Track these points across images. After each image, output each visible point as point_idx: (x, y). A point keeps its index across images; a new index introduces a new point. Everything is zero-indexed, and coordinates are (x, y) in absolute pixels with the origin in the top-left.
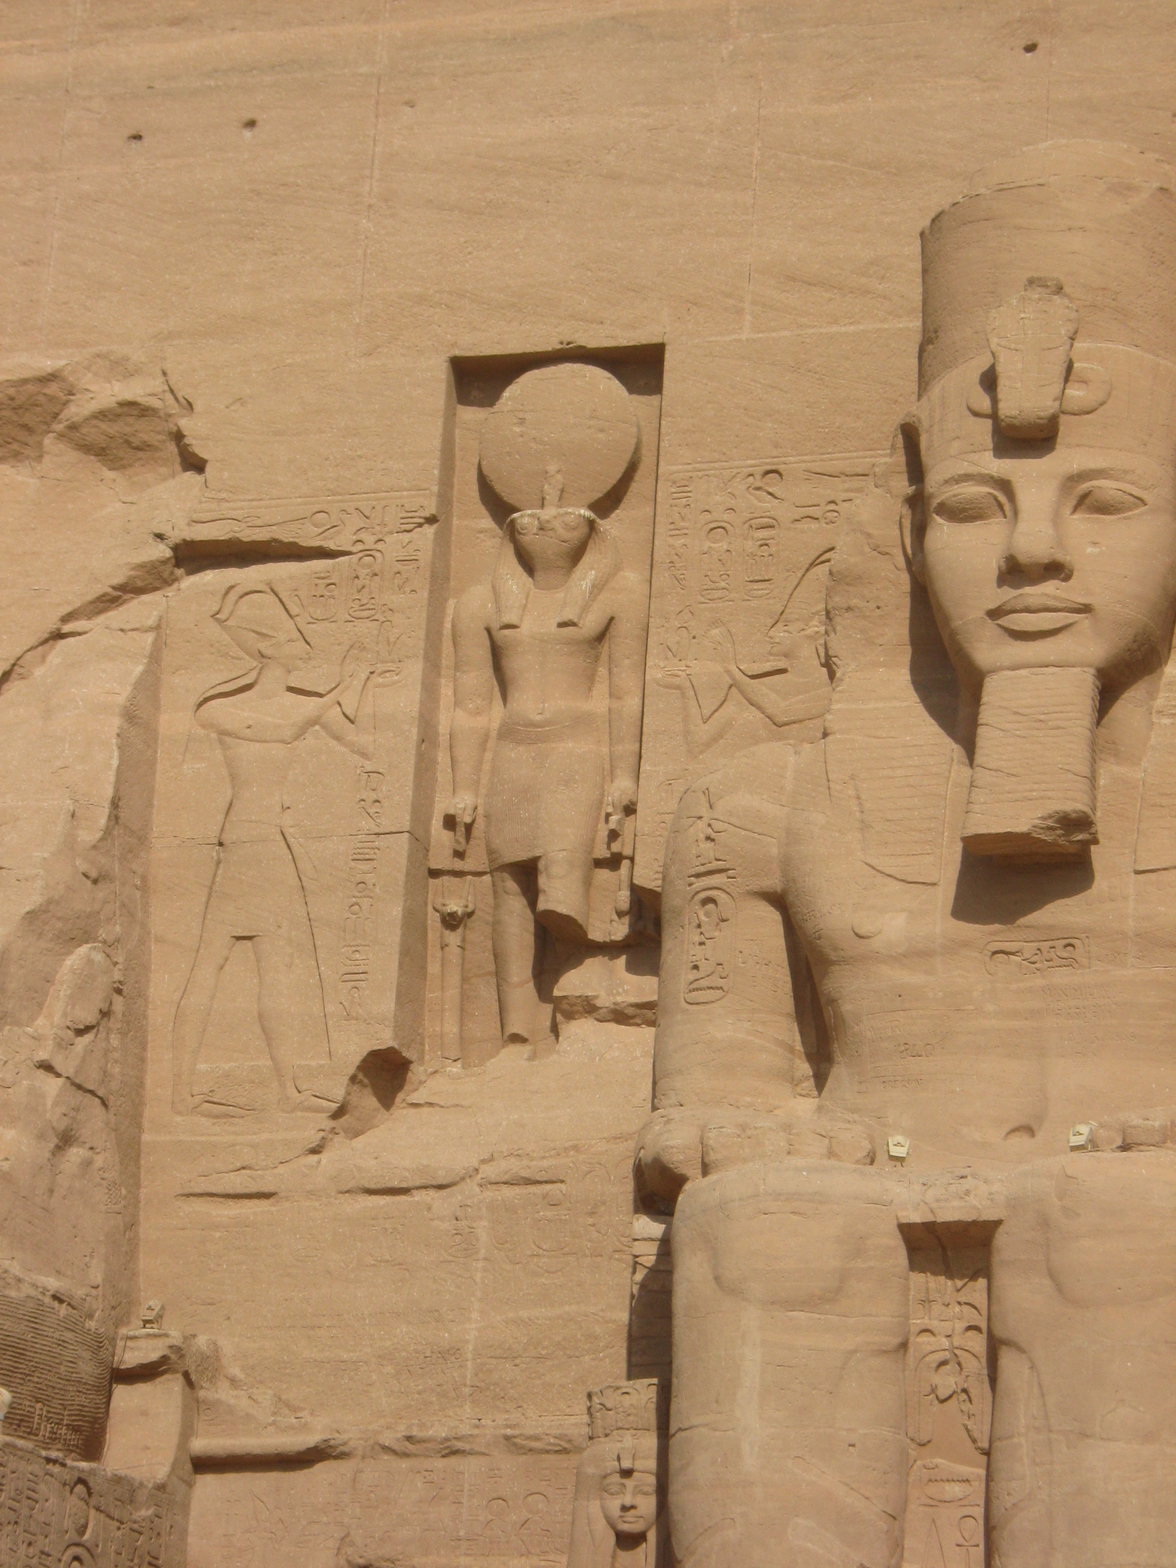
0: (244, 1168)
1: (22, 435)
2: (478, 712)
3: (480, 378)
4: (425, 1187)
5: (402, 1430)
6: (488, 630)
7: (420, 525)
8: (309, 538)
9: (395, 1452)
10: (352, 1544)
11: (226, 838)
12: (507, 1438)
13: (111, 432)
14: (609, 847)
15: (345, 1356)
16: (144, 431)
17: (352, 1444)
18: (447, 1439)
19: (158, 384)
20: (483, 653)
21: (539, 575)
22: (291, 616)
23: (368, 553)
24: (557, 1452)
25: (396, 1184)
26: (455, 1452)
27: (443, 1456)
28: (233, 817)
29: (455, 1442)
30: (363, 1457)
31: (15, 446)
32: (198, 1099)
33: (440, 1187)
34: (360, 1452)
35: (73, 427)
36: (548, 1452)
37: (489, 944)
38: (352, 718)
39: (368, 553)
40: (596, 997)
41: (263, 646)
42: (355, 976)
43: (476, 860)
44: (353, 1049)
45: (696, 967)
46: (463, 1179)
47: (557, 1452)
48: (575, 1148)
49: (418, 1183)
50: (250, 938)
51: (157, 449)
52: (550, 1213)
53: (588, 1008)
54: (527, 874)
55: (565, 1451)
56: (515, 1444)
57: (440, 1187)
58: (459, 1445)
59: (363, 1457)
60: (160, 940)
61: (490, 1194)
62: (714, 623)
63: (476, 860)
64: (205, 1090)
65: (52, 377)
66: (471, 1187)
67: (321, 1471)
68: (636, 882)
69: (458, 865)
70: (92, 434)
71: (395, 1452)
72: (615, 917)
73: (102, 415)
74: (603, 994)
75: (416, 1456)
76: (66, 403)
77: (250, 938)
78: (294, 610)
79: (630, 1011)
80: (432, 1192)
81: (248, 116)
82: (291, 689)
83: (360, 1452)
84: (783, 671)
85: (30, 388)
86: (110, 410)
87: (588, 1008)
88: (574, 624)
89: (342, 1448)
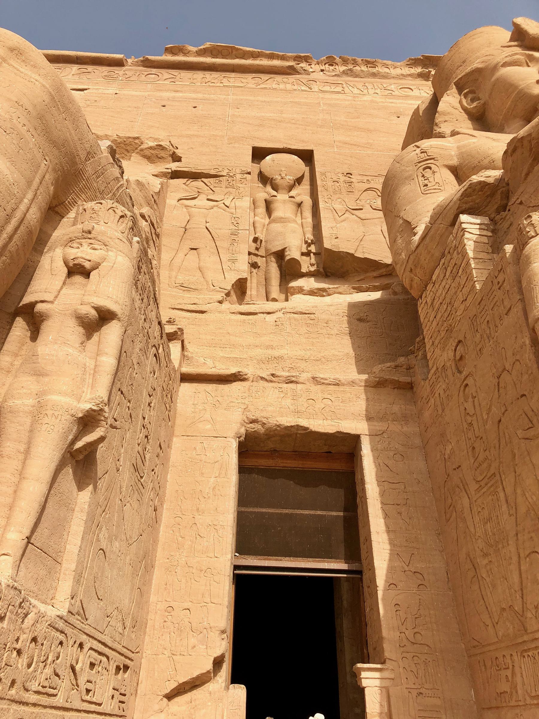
0: (194, 304)
1: (126, 153)
2: (262, 218)
3: (259, 154)
4: (263, 313)
5: (269, 373)
6: (266, 200)
7: (246, 174)
8: (212, 172)
9: (266, 380)
10: (249, 411)
11: (187, 227)
12: (313, 378)
13: (153, 152)
14: (307, 249)
15: (237, 357)
16: (162, 154)
17: (248, 375)
18: (289, 376)
19: (168, 144)
20: (263, 205)
21: (280, 191)
22: (208, 186)
23: (231, 176)
24: (334, 385)
25: (252, 311)
26: (292, 382)
27: (286, 383)
28: (189, 223)
29: (292, 378)
30: (253, 381)
31: (123, 155)
32: (177, 285)
33: (269, 313)
34: (251, 379)
35: (142, 150)
36: (330, 384)
37: (264, 277)
38: (228, 205)
39: (231, 176)
40: (304, 287)
41: (199, 191)
42: (234, 261)
43: (262, 252)
44: (232, 278)
45: (426, 185)
46: (277, 311)
47: (334, 385)
48: (316, 307)
49: (261, 311)
50: (196, 249)
51: (165, 159)
52: (311, 322)
53: (300, 290)
54: (280, 255)
55: (338, 385)
56: (317, 380)
57: (269, 313)
58: (293, 379)
59: (253, 381)
60: (164, 245)
61: (288, 315)
62: (339, 198)
63: (262, 252)
64: (181, 282)
65: (138, 138)
66: (280, 314)
67: (236, 385)
68: (327, 244)
69: (256, 252)
70: (147, 153)
71: (266, 380)
72: (309, 265)
73: (151, 148)
74: (306, 287)
75: (275, 382)
76: (140, 145)
77: (196, 249)
78: (208, 185)
79: (315, 291)
80: (265, 315)
81: (194, 106)
82: (208, 200)
83: (251, 379)
84: (361, 209)
85: (131, 140)
86: (153, 147)
87: (300, 290)
88: (294, 197)
89: (246, 377)
